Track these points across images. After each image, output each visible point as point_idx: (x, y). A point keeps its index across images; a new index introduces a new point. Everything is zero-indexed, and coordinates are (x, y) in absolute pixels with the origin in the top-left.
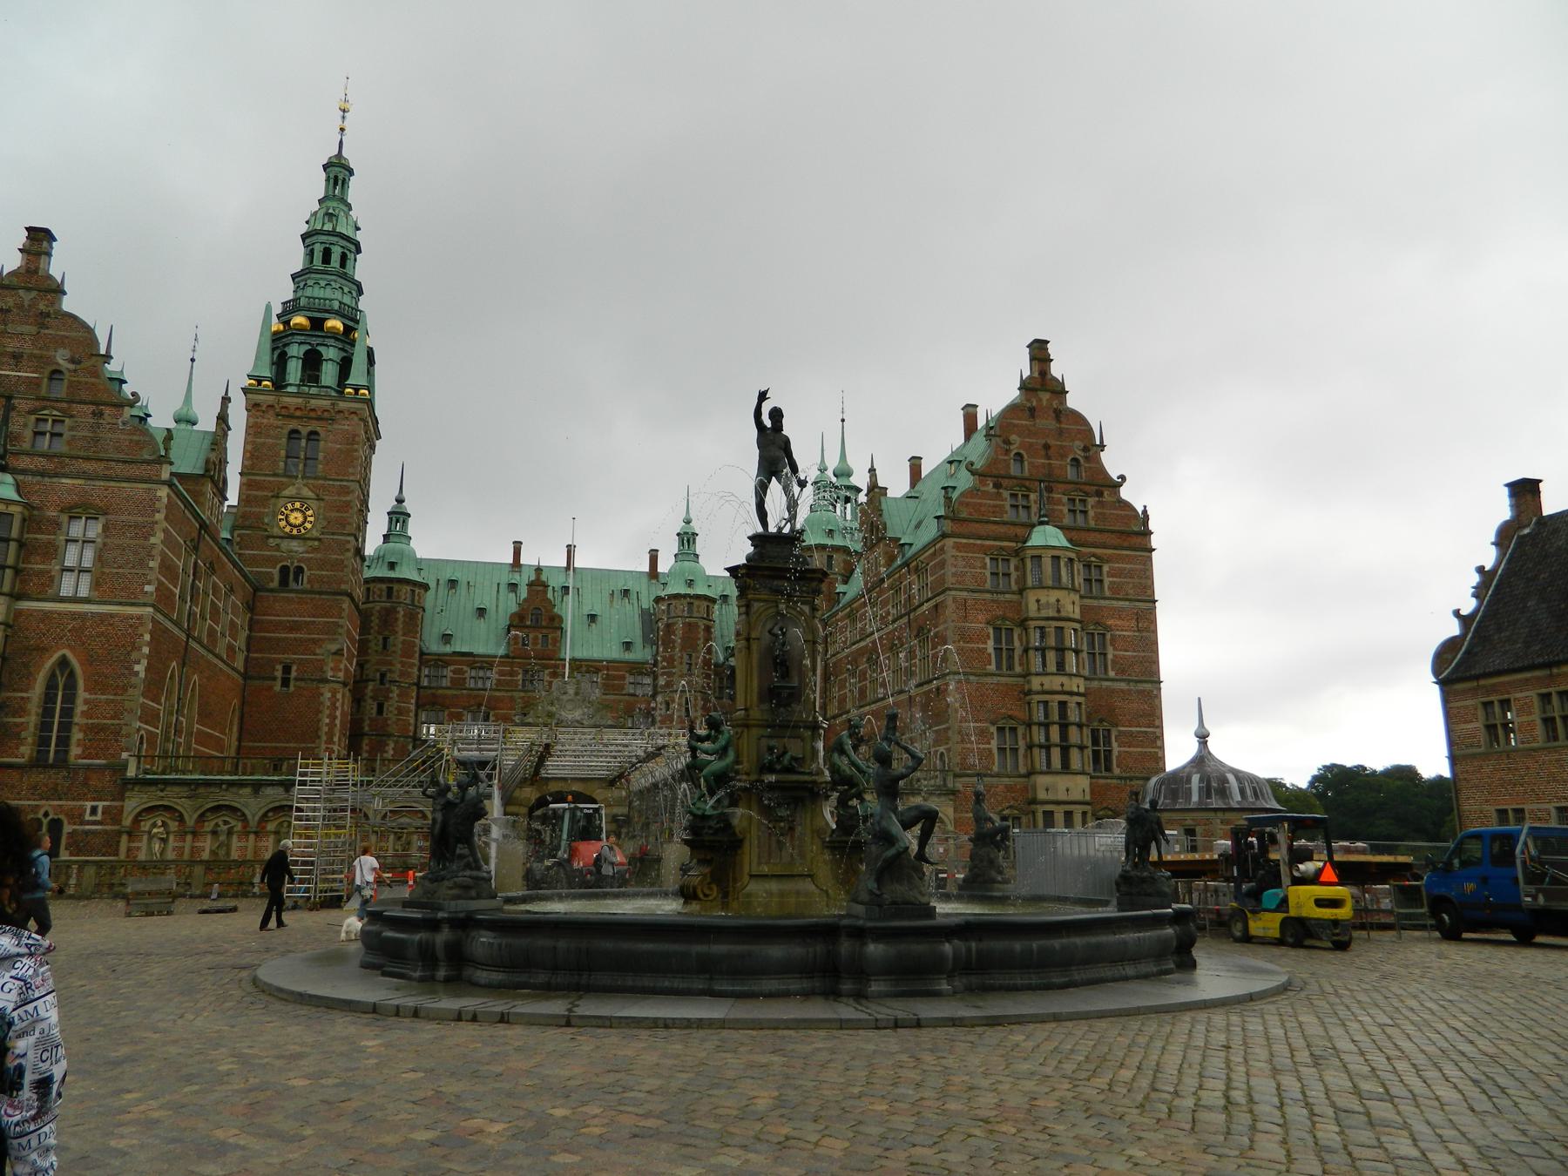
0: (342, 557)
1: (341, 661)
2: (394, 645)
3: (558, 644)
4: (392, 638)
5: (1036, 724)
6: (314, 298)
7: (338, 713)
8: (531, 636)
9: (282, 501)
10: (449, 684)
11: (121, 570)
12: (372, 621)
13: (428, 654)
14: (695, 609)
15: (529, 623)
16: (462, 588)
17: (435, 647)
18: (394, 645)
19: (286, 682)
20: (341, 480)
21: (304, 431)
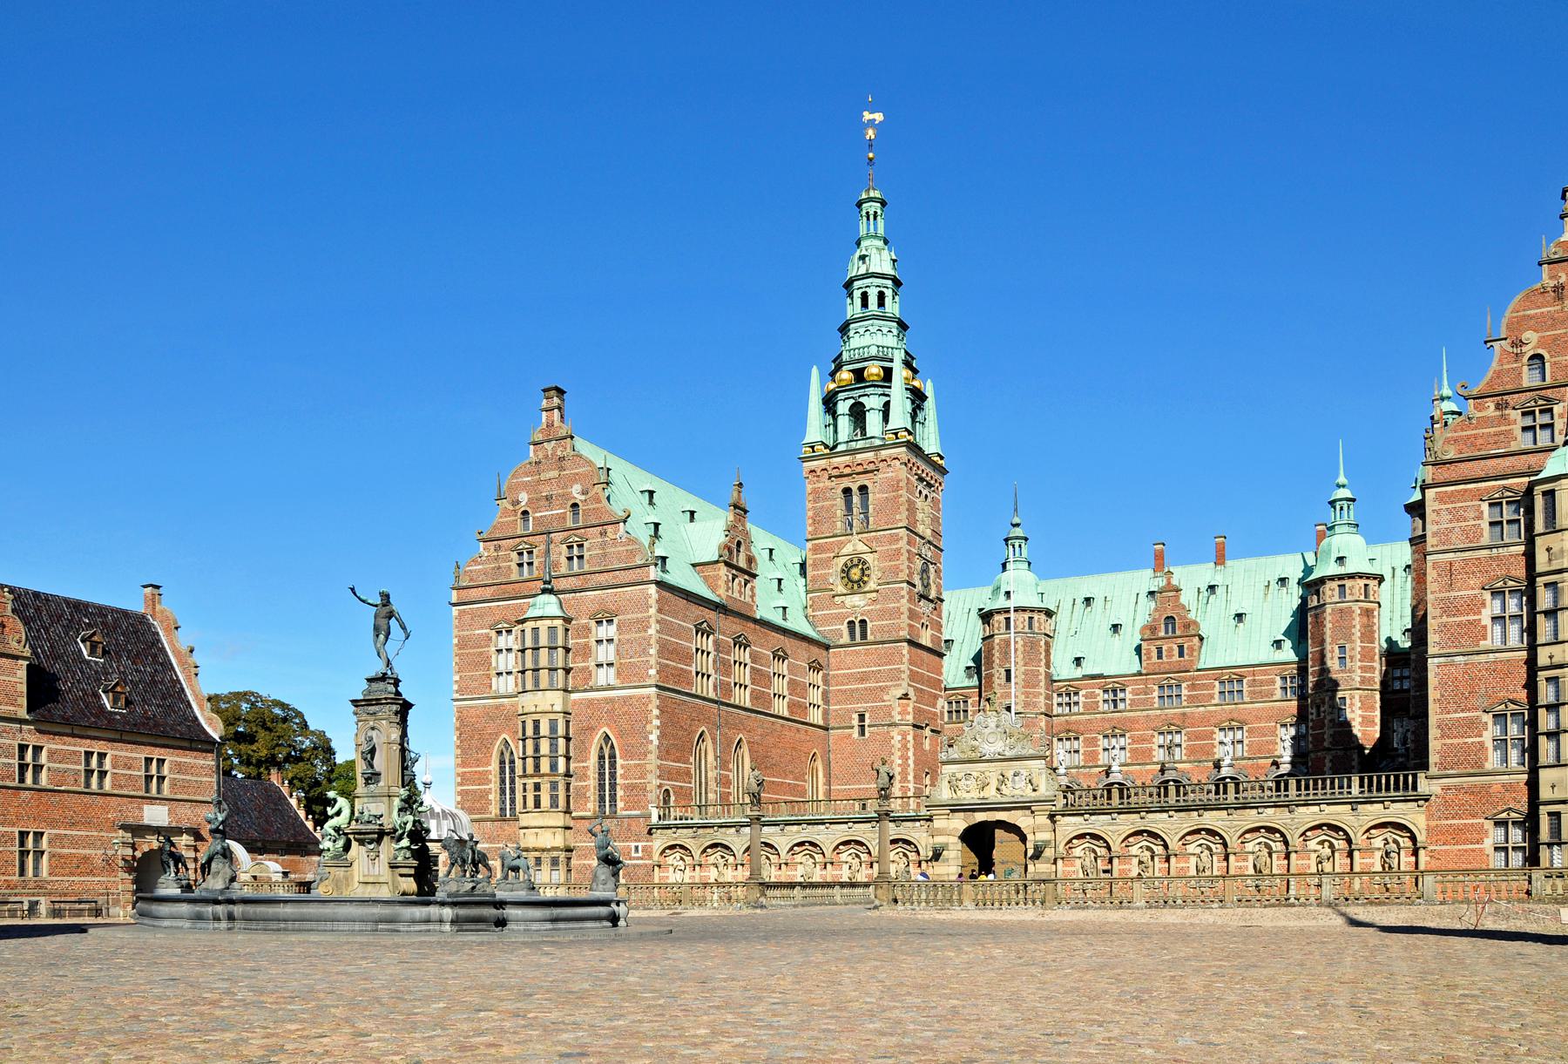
1: (908, 705)
3: (1195, 654)
5: (1542, 707)
7: (910, 754)
8: (1164, 648)
10: (1082, 710)
11: (632, 660)
13: (1059, 681)
14: (1348, 591)
15: (1162, 634)
16: (1098, 604)
17: (1063, 669)
19: (862, 733)
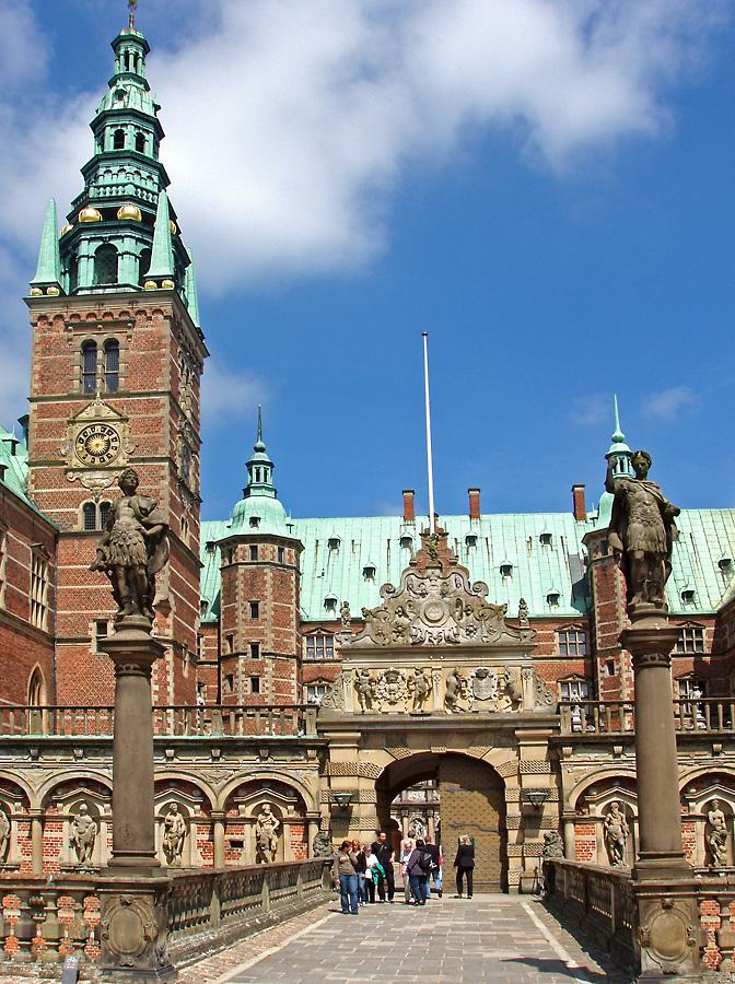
0: (154, 487)
2: (265, 612)
4: (260, 605)
6: (105, 187)
9: (80, 427)
12: (237, 587)
13: (310, 623)
16: (345, 546)
17: (314, 610)
18: (265, 612)
20: (148, 394)
21: (100, 340)
